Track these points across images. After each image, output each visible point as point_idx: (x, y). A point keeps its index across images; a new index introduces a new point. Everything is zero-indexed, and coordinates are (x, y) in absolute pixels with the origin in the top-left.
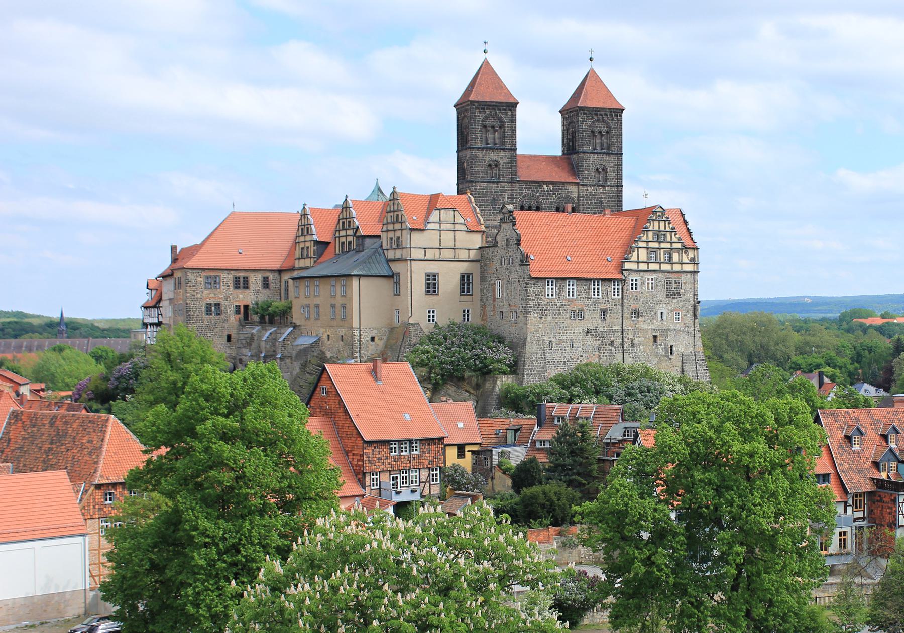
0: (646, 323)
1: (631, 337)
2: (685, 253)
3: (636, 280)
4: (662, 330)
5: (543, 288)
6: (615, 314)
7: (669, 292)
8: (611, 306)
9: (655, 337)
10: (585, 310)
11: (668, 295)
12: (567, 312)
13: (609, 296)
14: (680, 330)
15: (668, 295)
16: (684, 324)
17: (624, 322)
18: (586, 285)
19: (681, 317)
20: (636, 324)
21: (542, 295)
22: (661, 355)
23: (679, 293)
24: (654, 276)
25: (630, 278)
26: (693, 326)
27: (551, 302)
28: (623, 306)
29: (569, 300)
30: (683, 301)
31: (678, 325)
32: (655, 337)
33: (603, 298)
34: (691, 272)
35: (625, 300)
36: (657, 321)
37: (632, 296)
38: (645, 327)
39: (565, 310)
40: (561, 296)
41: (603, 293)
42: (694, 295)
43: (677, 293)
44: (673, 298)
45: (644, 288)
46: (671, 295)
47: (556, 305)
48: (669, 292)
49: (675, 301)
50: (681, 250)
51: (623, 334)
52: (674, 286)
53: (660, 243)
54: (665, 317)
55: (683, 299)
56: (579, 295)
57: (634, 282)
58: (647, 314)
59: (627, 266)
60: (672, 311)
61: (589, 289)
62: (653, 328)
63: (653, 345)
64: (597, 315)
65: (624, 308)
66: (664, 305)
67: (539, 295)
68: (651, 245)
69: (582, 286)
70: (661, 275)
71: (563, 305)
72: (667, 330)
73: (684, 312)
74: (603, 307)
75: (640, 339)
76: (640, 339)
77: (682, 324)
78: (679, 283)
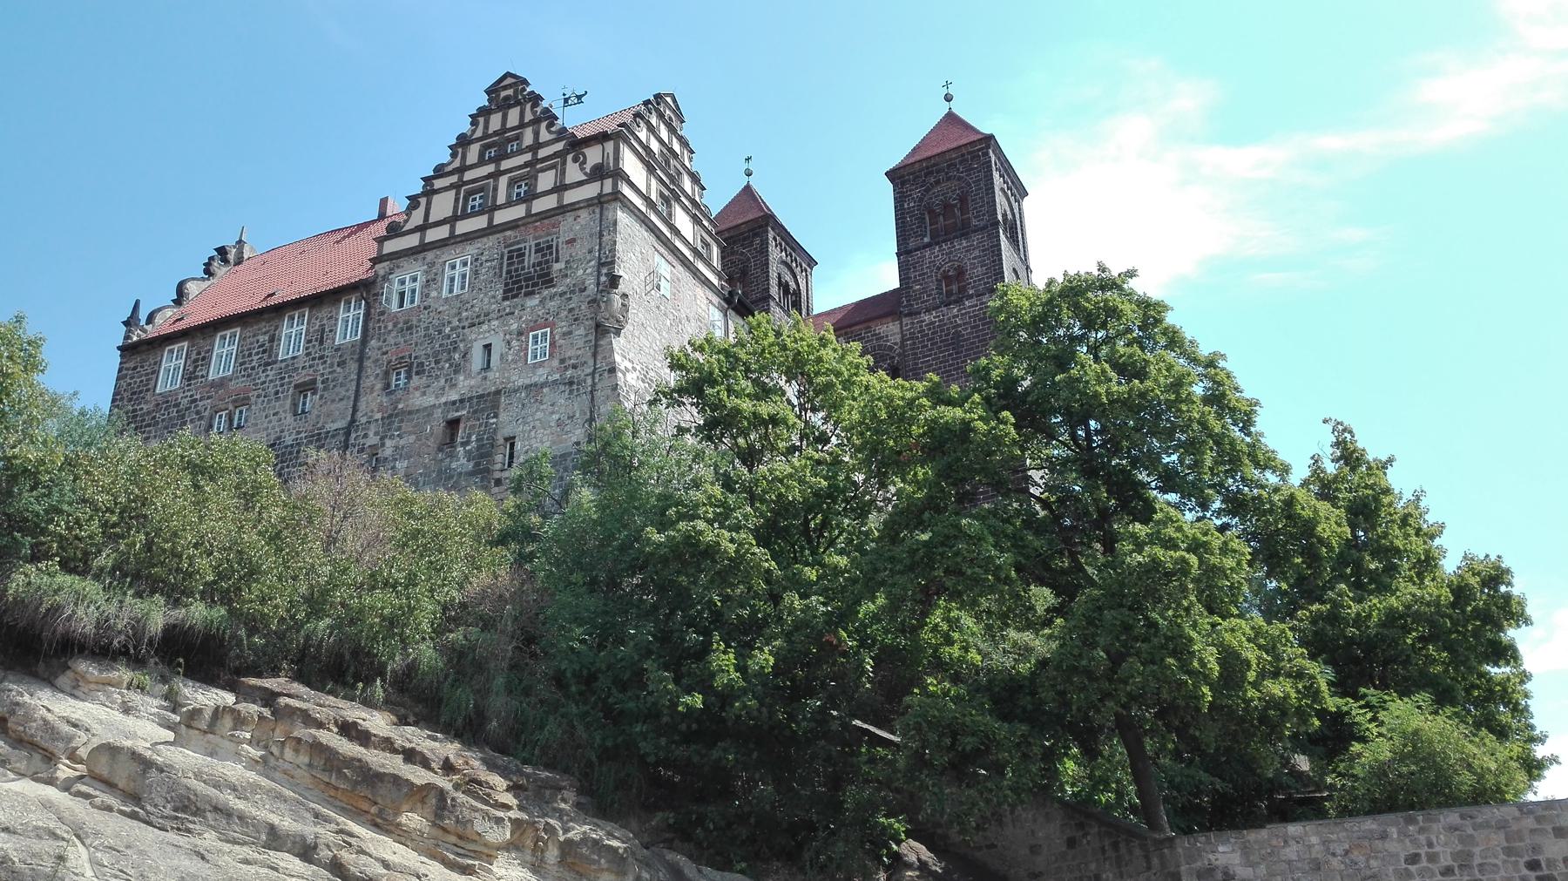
0: (431, 389)
1: (373, 440)
2: (575, 160)
3: (414, 279)
4: (482, 396)
5: (153, 373)
6: (338, 389)
7: (514, 283)
8: (328, 370)
9: (453, 424)
10: (253, 399)
11: (512, 290)
12: (201, 418)
13: (326, 345)
14: (543, 385)
15: (512, 290)
16: (562, 361)
17: (362, 406)
18: (265, 333)
19: (553, 344)
20: (399, 400)
21: (148, 390)
22: (461, 473)
23: (548, 274)
24: (471, 250)
25: (395, 278)
26: (591, 362)
27: (168, 400)
28: (361, 361)
29: (213, 384)
30: (561, 295)
31: (540, 371)
32: (453, 424)
33: (308, 354)
34: (589, 203)
35: (373, 343)
36: (468, 376)
37: (395, 325)
38: (430, 400)
39: (198, 413)
40: (196, 377)
41: (309, 341)
42: (601, 265)
43: (540, 276)
44: (532, 293)
45: (434, 294)
46: (520, 288)
47: (177, 405)
48: (514, 283)
49: (533, 302)
50: (560, 155)
51: (347, 440)
52: (531, 258)
53: (497, 160)
54: (495, 358)
55: (561, 289)
56: (241, 364)
57: (408, 286)
58: (437, 362)
59: (391, 246)
60: (520, 333)
61: (272, 340)
62: (454, 396)
63: (440, 450)
64: (281, 406)
65: (367, 363)
66: (496, 323)
67: (141, 392)
68: (468, 176)
69: (255, 339)
70: (490, 241)
71: (196, 400)
72: (498, 392)
73: (562, 326)
74: (299, 378)
75: (402, 442)
76: (402, 442)
77: (555, 363)
78: (550, 247)
